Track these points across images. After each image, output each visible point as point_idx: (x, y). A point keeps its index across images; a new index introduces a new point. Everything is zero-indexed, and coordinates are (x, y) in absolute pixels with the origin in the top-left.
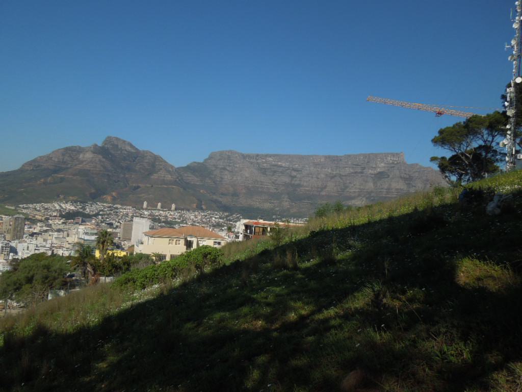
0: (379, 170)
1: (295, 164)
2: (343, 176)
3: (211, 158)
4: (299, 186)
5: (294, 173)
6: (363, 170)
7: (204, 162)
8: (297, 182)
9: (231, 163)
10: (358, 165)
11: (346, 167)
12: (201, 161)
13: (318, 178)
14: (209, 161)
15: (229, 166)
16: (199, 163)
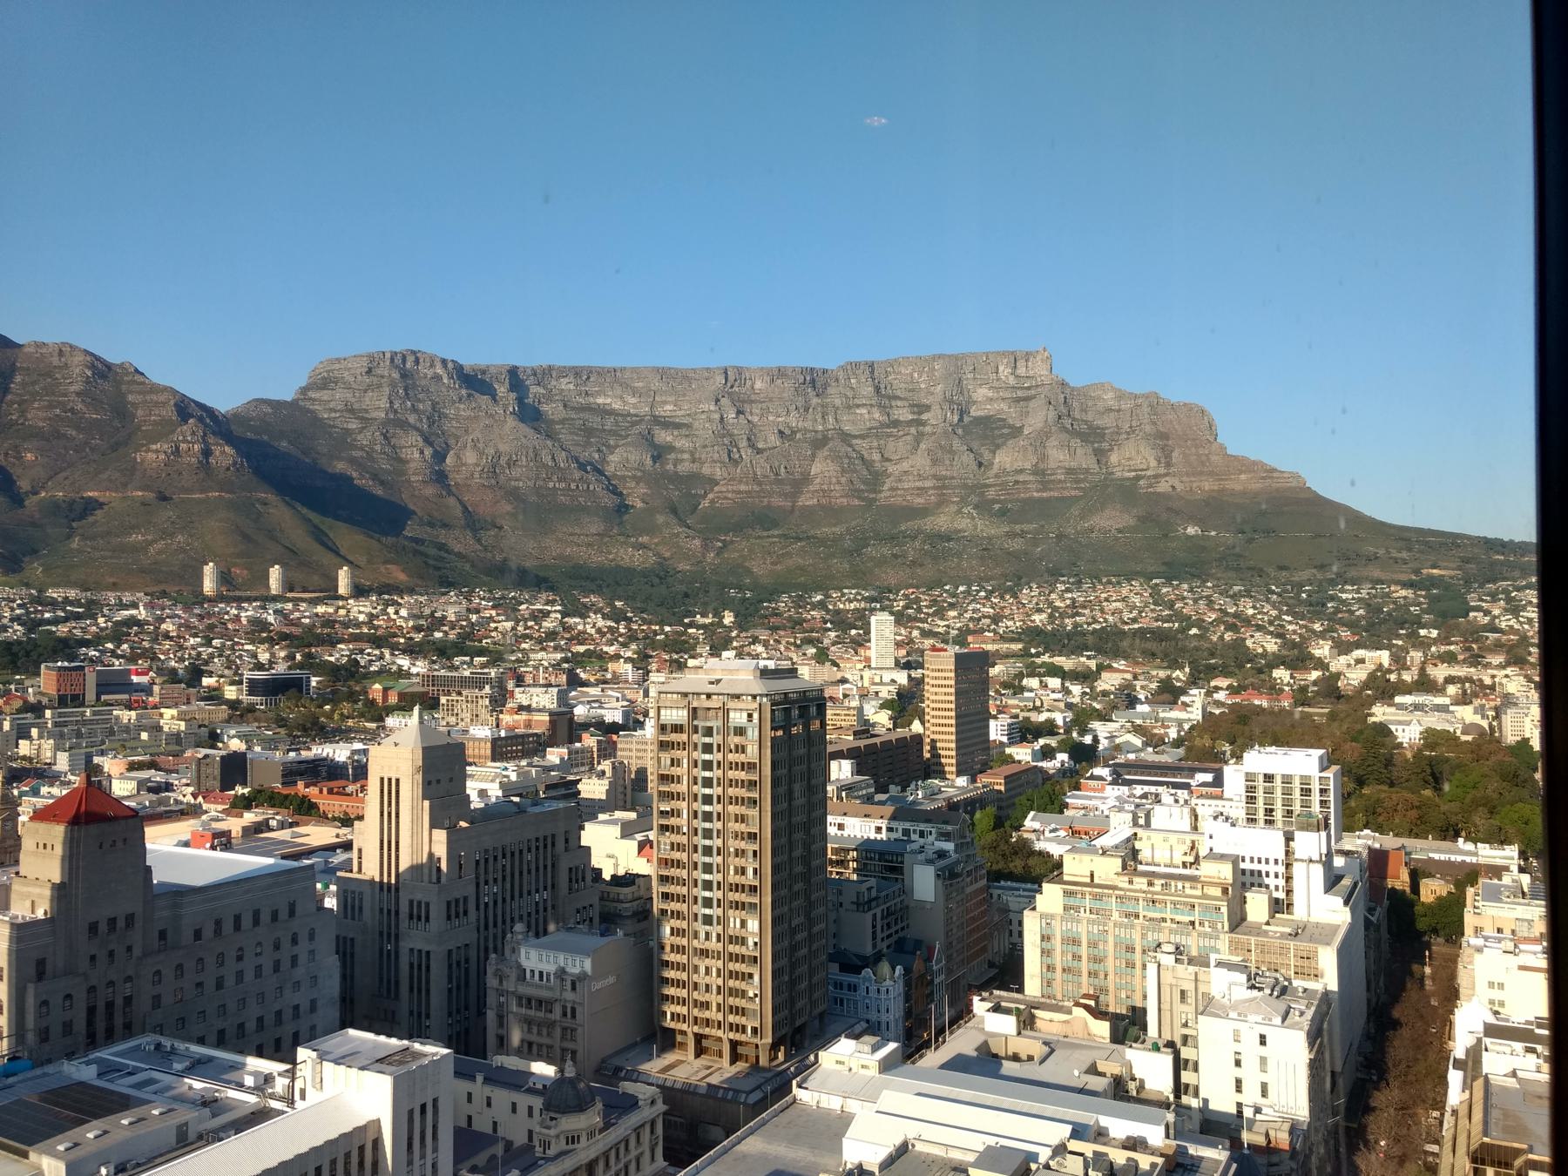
0: (975, 412)
1: (665, 403)
2: (855, 437)
3: (324, 382)
4: (694, 478)
5: (664, 437)
6: (920, 413)
7: (293, 405)
8: (685, 468)
9: (419, 401)
10: (897, 398)
11: (858, 406)
12: (287, 394)
13: (759, 451)
14: (324, 395)
15: (414, 409)
16: (277, 405)
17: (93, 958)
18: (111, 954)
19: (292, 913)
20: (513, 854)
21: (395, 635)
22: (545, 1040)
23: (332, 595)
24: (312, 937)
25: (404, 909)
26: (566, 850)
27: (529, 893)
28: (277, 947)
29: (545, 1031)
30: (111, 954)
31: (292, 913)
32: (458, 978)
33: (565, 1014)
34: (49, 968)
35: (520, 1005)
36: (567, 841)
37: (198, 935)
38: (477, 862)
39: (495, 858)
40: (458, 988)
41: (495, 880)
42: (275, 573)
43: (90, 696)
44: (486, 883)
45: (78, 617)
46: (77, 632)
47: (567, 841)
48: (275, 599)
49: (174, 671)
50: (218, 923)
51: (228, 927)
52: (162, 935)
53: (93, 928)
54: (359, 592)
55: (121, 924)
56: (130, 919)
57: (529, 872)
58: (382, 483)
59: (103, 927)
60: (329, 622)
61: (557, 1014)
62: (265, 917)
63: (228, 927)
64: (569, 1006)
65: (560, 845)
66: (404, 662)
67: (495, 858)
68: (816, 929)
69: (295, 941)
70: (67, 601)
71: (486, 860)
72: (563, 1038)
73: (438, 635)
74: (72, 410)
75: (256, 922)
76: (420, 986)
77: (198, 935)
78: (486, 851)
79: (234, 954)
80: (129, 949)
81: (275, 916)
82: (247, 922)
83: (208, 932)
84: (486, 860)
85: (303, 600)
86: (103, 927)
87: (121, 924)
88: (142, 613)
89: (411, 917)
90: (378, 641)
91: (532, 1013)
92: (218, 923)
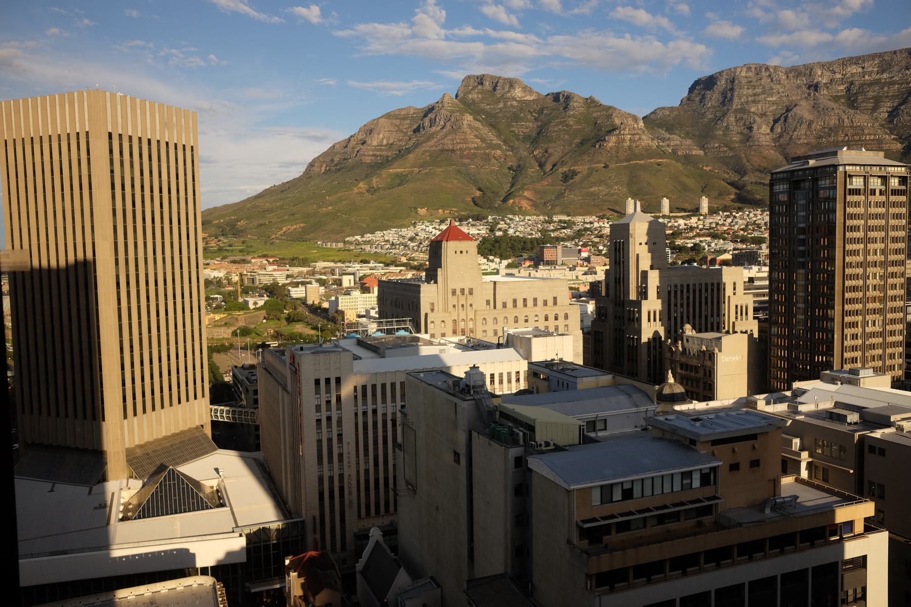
17: (454, 306)
18: (463, 306)
19: (555, 303)
20: (694, 291)
21: (728, 234)
22: (696, 390)
23: (696, 211)
24: (566, 317)
25: (626, 315)
26: (734, 294)
27: (706, 316)
28: (546, 319)
29: (695, 384)
30: (463, 306)
31: (555, 303)
32: (655, 356)
33: (705, 374)
34: (436, 308)
35: (681, 369)
36: (734, 289)
37: (504, 305)
38: (669, 292)
39: (682, 292)
40: (655, 361)
41: (682, 305)
42: (666, 202)
43: (559, 262)
44: (676, 305)
45: (564, 228)
46: (562, 235)
47: (734, 289)
48: (664, 217)
49: (601, 251)
50: (515, 301)
51: (520, 303)
52: (488, 302)
53: (454, 293)
54: (712, 211)
55: (467, 292)
56: (471, 293)
57: (706, 303)
58: (731, 149)
59: (458, 292)
60: (692, 229)
61: (701, 374)
62: (540, 302)
63: (520, 303)
64: (707, 369)
65: (729, 291)
66: (731, 246)
67: (682, 292)
68: (890, 339)
69: (556, 318)
70: (560, 221)
71: (676, 292)
72: (704, 389)
73: (756, 234)
74: (567, 126)
75: (535, 305)
76: (634, 360)
77: (504, 305)
78: (676, 286)
79: (524, 318)
80: (471, 305)
81: (545, 303)
82: (530, 303)
83: (510, 304)
84: (676, 292)
85: (677, 217)
86: (458, 292)
87: (467, 292)
88: (596, 225)
89: (629, 319)
90: (715, 236)
91: (688, 373)
92: (515, 301)
